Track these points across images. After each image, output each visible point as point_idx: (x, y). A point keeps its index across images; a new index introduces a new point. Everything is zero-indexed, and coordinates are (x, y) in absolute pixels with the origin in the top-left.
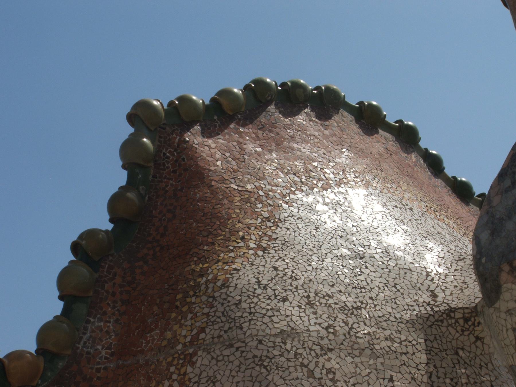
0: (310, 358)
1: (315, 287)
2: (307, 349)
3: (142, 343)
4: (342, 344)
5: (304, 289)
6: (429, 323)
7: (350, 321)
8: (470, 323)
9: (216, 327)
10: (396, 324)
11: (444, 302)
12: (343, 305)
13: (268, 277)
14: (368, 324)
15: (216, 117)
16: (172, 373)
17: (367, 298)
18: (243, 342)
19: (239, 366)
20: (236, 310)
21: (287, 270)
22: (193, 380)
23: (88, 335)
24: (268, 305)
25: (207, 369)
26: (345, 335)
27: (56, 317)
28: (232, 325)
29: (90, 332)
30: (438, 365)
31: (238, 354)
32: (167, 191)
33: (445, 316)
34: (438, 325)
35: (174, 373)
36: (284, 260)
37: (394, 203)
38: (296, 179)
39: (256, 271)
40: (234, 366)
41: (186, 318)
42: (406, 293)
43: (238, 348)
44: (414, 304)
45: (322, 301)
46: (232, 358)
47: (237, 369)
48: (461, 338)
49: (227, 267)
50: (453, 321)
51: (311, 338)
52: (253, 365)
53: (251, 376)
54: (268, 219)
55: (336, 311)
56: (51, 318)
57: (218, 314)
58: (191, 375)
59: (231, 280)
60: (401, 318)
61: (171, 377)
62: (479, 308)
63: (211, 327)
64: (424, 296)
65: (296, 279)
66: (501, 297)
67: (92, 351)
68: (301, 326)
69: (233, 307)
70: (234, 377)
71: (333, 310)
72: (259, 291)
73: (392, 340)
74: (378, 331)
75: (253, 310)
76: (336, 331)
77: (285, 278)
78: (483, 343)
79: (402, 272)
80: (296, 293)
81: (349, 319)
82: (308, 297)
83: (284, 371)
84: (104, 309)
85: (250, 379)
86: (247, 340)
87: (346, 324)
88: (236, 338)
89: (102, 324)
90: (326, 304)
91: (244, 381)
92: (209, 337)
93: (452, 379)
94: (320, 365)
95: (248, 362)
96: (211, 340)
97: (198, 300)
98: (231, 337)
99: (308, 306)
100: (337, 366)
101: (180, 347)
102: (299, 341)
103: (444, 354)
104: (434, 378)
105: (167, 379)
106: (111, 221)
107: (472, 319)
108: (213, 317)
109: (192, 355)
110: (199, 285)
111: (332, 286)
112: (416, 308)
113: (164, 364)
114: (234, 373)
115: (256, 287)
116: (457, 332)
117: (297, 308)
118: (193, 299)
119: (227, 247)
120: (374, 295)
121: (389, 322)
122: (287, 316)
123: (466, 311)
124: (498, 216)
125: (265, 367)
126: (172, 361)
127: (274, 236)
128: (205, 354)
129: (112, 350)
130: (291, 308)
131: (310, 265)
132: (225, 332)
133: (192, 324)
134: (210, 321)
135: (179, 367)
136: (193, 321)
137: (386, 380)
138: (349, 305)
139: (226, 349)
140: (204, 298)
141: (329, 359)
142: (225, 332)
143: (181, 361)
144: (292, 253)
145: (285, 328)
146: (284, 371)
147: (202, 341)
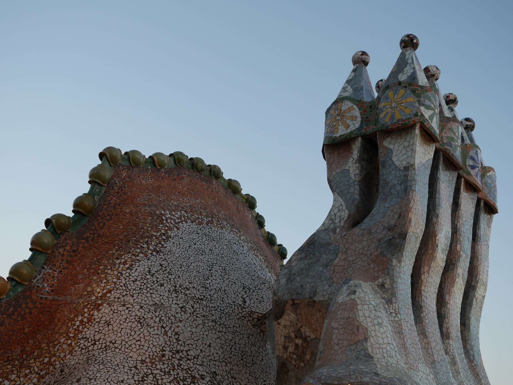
0: (168, 324)
1: (181, 282)
2: (167, 318)
3: (72, 289)
4: (188, 319)
5: (174, 281)
6: (238, 317)
7: (195, 306)
8: (260, 322)
10: (220, 313)
11: (249, 307)
12: (194, 295)
13: (155, 269)
14: (205, 310)
15: (149, 168)
16: (85, 312)
17: (208, 294)
18: (132, 305)
20: (132, 285)
21: (167, 268)
22: (96, 320)
23: (41, 276)
24: (152, 286)
25: (106, 316)
26: (190, 314)
27: (25, 261)
30: (237, 342)
31: (127, 311)
32: (110, 203)
33: (248, 315)
35: (86, 312)
36: (167, 261)
37: (234, 241)
38: (185, 214)
39: (150, 264)
40: (123, 318)
41: (102, 281)
42: (230, 296)
43: (127, 308)
44: (233, 304)
45: (183, 291)
46: (123, 313)
47: (124, 320)
48: (253, 329)
49: (134, 257)
50: (251, 319)
51: (171, 312)
52: (134, 320)
53: (131, 326)
54: (164, 234)
55: (189, 299)
56: (21, 261)
57: (121, 284)
58: (96, 317)
59: (134, 266)
60: (223, 311)
61: (83, 315)
62: (267, 315)
63: (115, 291)
64: (239, 300)
65: (171, 274)
66: (283, 317)
68: (167, 303)
69: (131, 282)
70: (121, 324)
71: (188, 297)
72: (148, 277)
73: (216, 322)
74: (209, 315)
75: (142, 287)
76: (186, 310)
77: (165, 272)
78: (264, 334)
79: (230, 283)
80: (169, 283)
81: (195, 305)
82: (176, 287)
83: (151, 328)
85: (130, 328)
86: (134, 305)
87: (193, 307)
89: (51, 271)
90: (184, 293)
91: (126, 329)
92: (112, 296)
93: (242, 352)
94: (172, 329)
95: (131, 318)
97: (112, 273)
98: (125, 300)
99: (174, 292)
100: (181, 332)
101: (94, 298)
102: (164, 311)
103: (241, 336)
104: (233, 349)
106: (73, 211)
107: (262, 320)
111: (190, 283)
112: (233, 306)
113: (82, 305)
115: (148, 274)
117: (167, 292)
118: (109, 272)
119: (137, 245)
120: (212, 294)
121: (216, 311)
122: (161, 295)
123: (260, 315)
124: (293, 272)
125: (141, 323)
126: (87, 305)
127: (165, 245)
130: (164, 291)
131: (181, 268)
132: (123, 296)
135: (90, 310)
136: (106, 285)
137: (207, 345)
138: (197, 296)
141: (178, 327)
142: (123, 296)
143: (92, 307)
144: (172, 258)
145: (158, 302)
146: (151, 328)
147: (107, 298)
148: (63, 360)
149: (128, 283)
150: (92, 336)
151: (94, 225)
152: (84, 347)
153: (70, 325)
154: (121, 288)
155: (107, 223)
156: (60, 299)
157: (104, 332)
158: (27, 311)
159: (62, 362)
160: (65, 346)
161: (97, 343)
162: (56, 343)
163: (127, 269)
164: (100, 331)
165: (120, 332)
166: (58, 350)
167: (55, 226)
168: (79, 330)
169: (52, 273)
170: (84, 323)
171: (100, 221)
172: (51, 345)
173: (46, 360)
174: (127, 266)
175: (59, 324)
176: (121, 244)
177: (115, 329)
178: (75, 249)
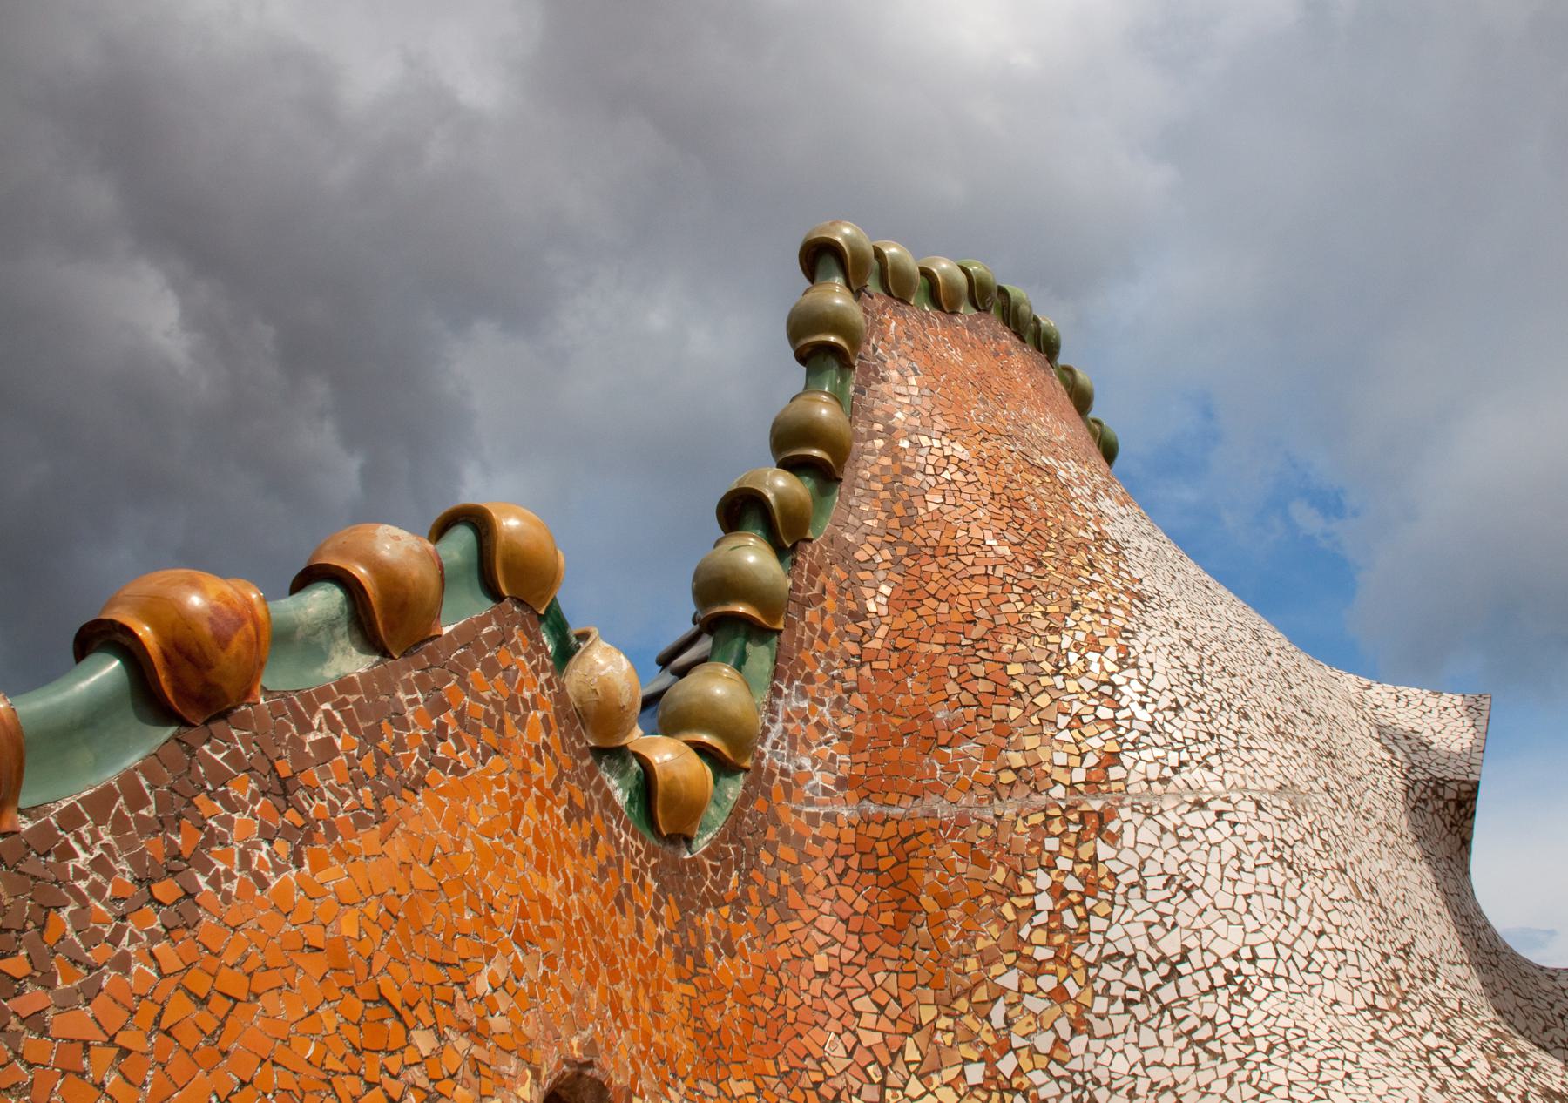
3: (934, 769)
8: (1462, 811)
18: (1228, 801)
19: (1237, 857)
23: (779, 726)
28: (1185, 756)
31: (1223, 826)
33: (1429, 791)
43: (1219, 814)
46: (1214, 836)
50: (1441, 804)
52: (1265, 859)
58: (1116, 867)
63: (1134, 754)
69: (1170, 715)
84: (808, 669)
85: (1272, 890)
89: (805, 704)
96: (1145, 785)
97: (1072, 686)
98: (1195, 786)
101: (1058, 792)
105: (1042, 867)
108: (1129, 731)
109: (1102, 818)
114: (1230, 872)
118: (1058, 680)
128: (1138, 818)
132: (1174, 770)
134: (1126, 741)
140: (1089, 685)
142: (1174, 770)
148: (1062, 1064)
149: (1159, 717)
150: (1142, 943)
152: (1136, 995)
153: (1007, 911)
154: (1143, 739)
155: (917, 501)
156: (897, 812)
157: (1182, 920)
158: (786, 878)
159: (1057, 1070)
160: (1035, 1004)
161: (1184, 968)
162: (981, 994)
164: (1169, 921)
165: (1248, 911)
166: (1009, 1023)
168: (1063, 929)
170: (1074, 898)
172: (962, 1004)
173: (976, 1073)
175: (953, 913)
176: (1020, 576)
177: (1224, 901)
178: (853, 606)
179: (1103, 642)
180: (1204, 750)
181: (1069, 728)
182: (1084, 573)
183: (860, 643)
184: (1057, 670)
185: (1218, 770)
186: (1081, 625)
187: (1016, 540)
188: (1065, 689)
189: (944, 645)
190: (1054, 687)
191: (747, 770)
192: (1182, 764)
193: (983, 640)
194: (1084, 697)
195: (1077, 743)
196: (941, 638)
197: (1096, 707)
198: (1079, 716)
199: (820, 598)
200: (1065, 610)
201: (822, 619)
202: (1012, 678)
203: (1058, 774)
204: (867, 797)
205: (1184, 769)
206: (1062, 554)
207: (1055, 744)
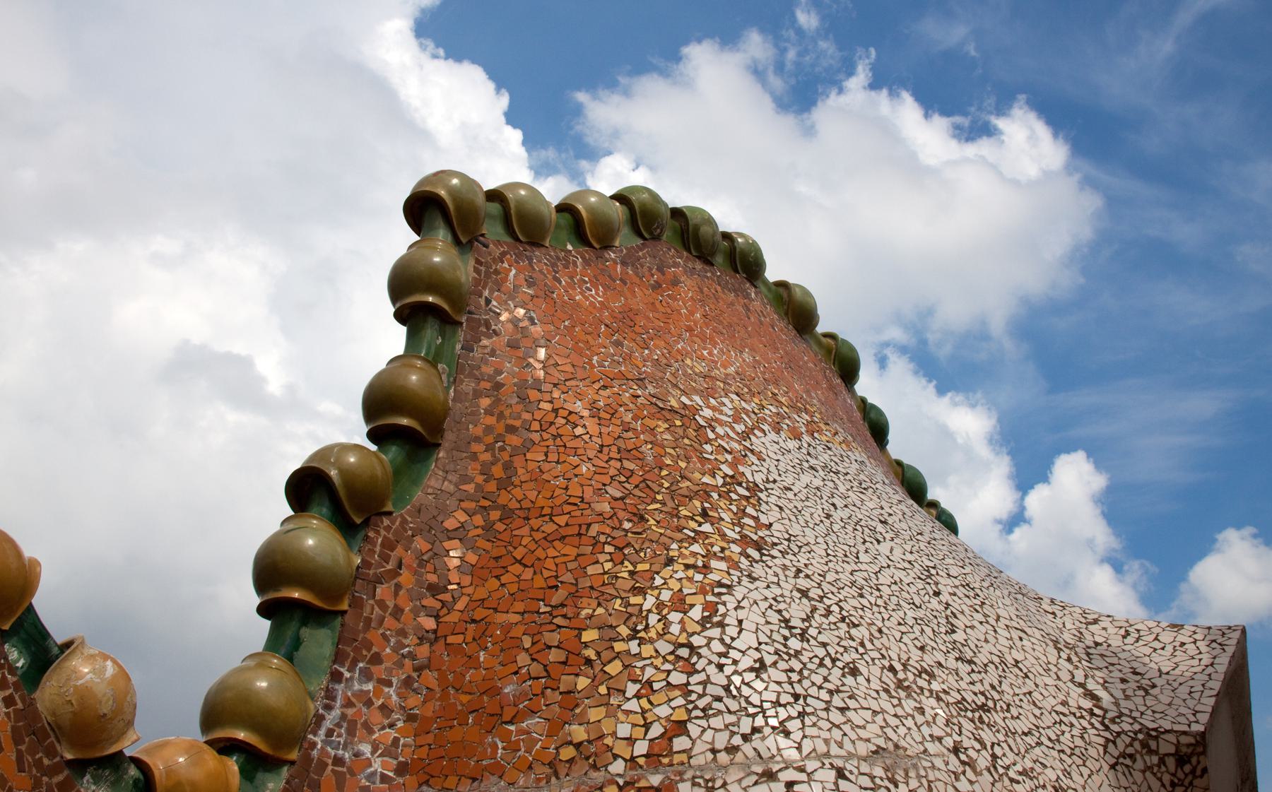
3: (495, 747)
8: (1187, 768)
9: (717, 722)
15: (570, 247)
18: (801, 770)
20: (759, 685)
23: (336, 712)
28: (759, 721)
29: (343, 706)
33: (1137, 745)
34: (1127, 766)
50: (1155, 759)
63: (703, 723)
67: (347, 755)
69: (749, 676)
72: (794, 644)
84: (375, 649)
88: (778, 758)
89: (369, 687)
96: (710, 756)
97: (647, 650)
98: (765, 755)
101: (618, 767)
107: (1194, 760)
108: (700, 696)
110: (642, 615)
116: (1163, 785)
118: (633, 646)
123: (1184, 740)
129: (401, 759)
132: (746, 738)
133: (644, 712)
134: (696, 707)
139: (756, 783)
140: (664, 647)
142: (746, 738)
149: (737, 680)
151: (466, 479)
154: (716, 705)
155: (518, 462)
163: (704, 622)
167: (342, 493)
169: (378, 693)
171: (486, 457)
174: (696, 613)
176: (617, 534)
178: (433, 578)
179: (689, 600)
180: (783, 714)
181: (638, 696)
182: (693, 524)
183: (437, 617)
184: (634, 634)
185: (797, 736)
186: (671, 580)
187: (619, 495)
188: (640, 653)
189: (522, 614)
190: (628, 652)
191: (292, 763)
192: (755, 730)
193: (563, 605)
194: (658, 662)
195: (644, 712)
196: (520, 606)
197: (669, 672)
198: (649, 683)
199: (395, 573)
200: (655, 568)
201: (396, 594)
202: (586, 645)
203: (620, 748)
204: (427, 783)
205: (757, 735)
206: (670, 504)
207: (620, 715)
